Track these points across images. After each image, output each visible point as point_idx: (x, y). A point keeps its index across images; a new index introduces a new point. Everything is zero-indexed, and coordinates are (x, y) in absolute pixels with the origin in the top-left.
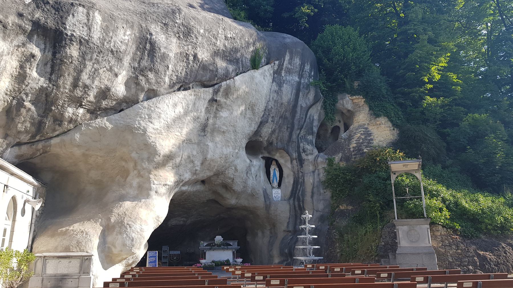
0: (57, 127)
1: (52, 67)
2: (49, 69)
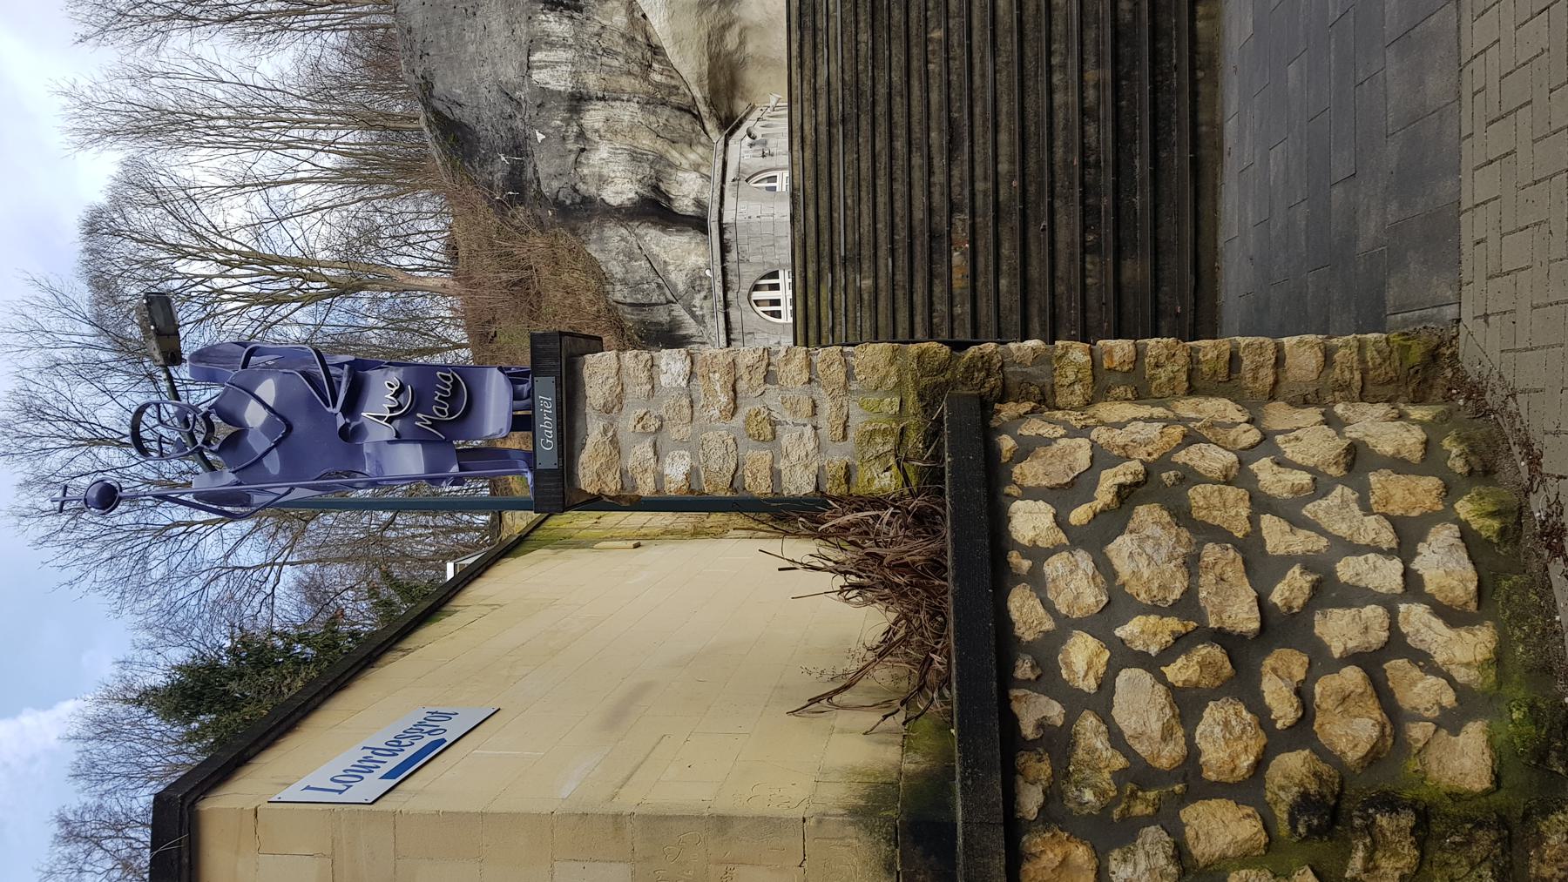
0: (681, 91)
1: (615, 100)
2: (618, 103)
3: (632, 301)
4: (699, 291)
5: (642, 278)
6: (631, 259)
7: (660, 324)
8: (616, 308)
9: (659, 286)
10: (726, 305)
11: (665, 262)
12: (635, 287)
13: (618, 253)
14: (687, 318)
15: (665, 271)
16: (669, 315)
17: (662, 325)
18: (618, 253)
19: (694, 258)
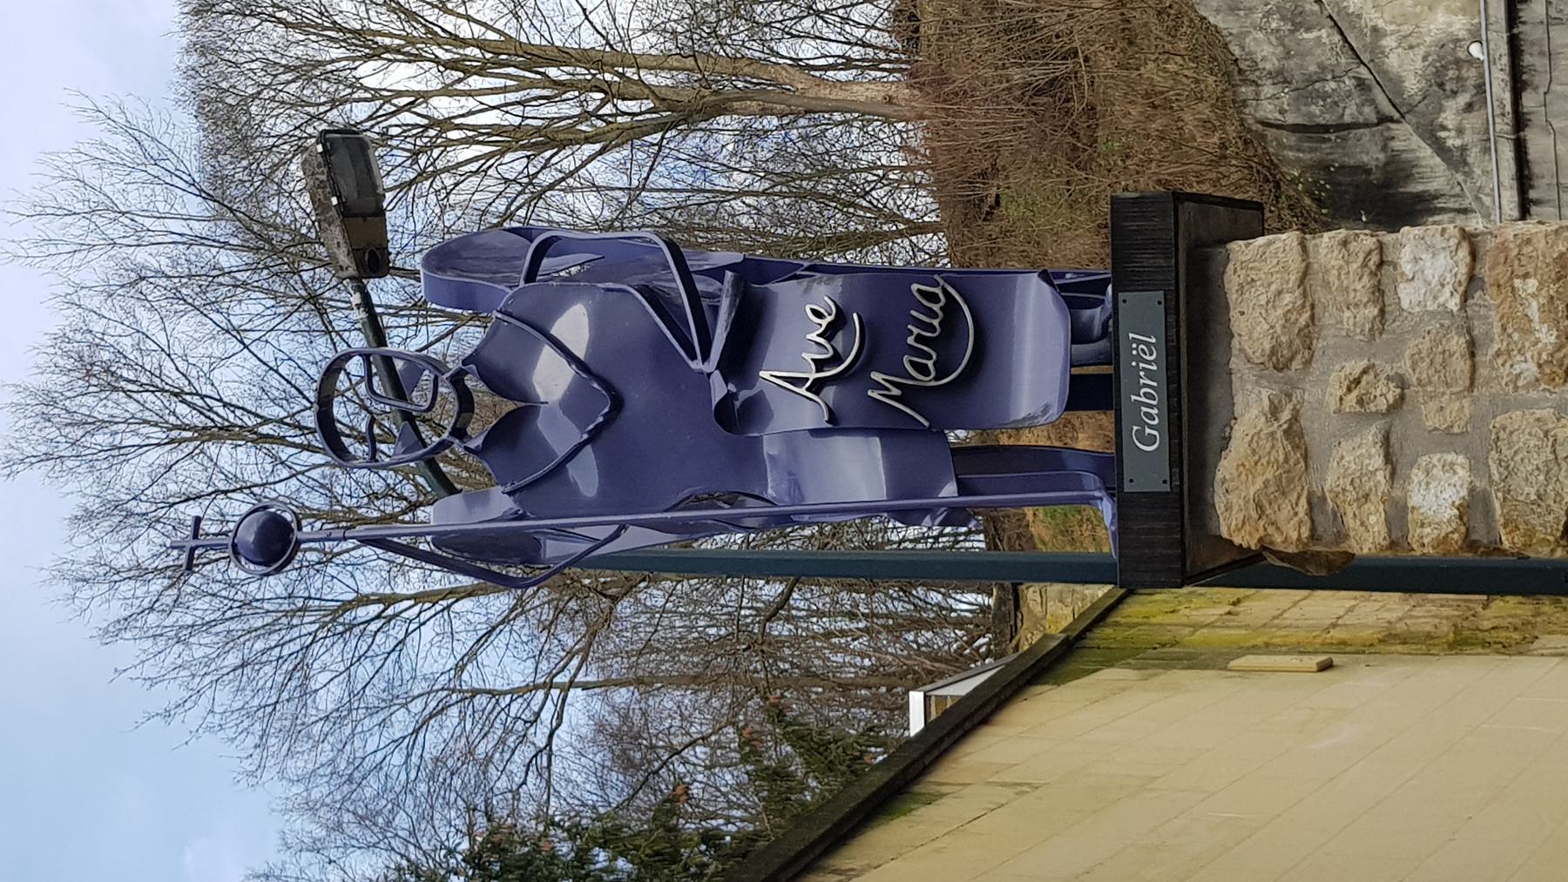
3: (1300, 121)
4: (1454, 93)
5: (1322, 67)
6: (1297, 27)
7: (1364, 170)
8: (1263, 137)
9: (1361, 84)
10: (1520, 121)
11: (1375, 29)
12: (1307, 89)
13: (1267, 15)
14: (1426, 154)
15: (1377, 51)
16: (1384, 148)
17: (1368, 172)
18: (1267, 15)
19: (1441, 18)
